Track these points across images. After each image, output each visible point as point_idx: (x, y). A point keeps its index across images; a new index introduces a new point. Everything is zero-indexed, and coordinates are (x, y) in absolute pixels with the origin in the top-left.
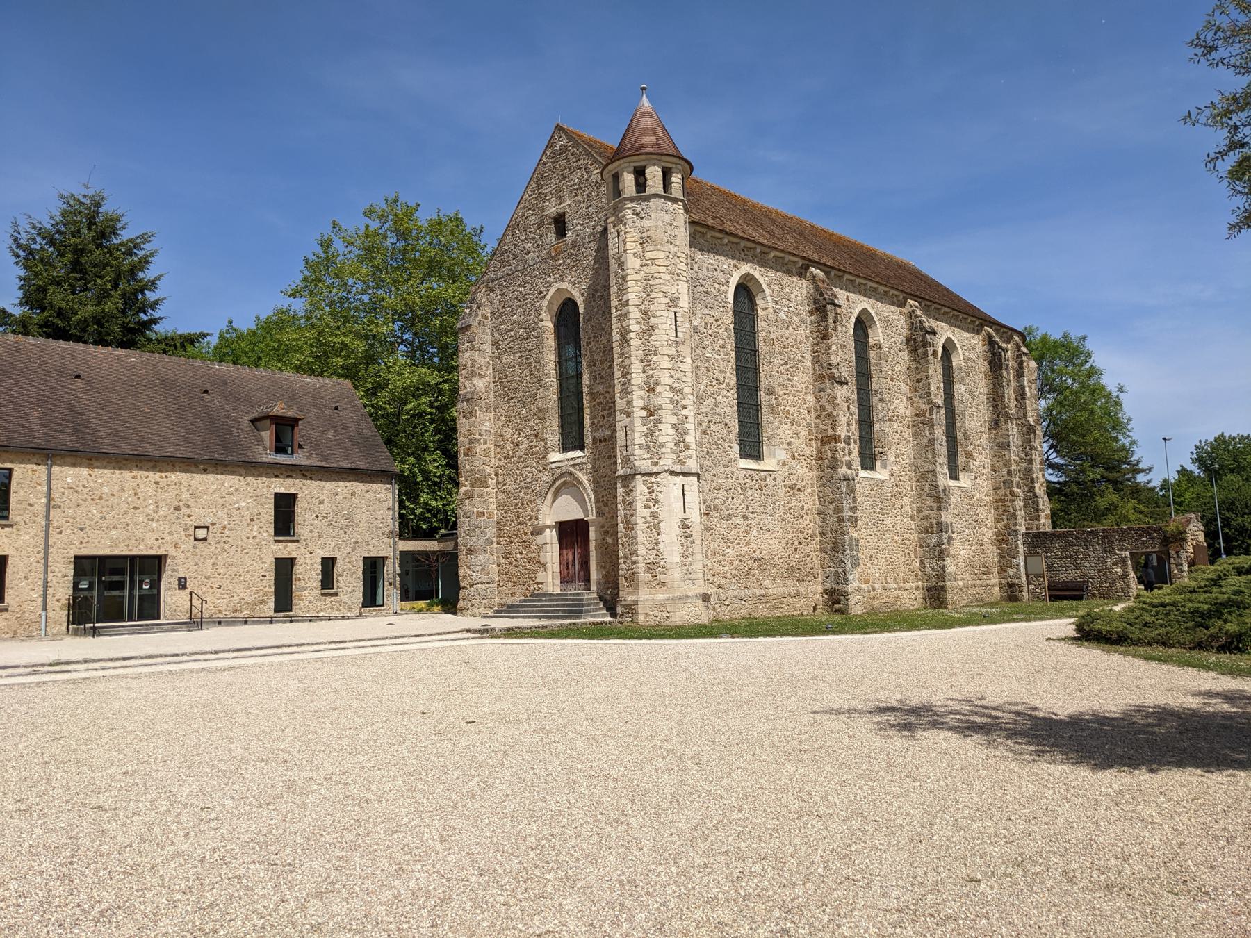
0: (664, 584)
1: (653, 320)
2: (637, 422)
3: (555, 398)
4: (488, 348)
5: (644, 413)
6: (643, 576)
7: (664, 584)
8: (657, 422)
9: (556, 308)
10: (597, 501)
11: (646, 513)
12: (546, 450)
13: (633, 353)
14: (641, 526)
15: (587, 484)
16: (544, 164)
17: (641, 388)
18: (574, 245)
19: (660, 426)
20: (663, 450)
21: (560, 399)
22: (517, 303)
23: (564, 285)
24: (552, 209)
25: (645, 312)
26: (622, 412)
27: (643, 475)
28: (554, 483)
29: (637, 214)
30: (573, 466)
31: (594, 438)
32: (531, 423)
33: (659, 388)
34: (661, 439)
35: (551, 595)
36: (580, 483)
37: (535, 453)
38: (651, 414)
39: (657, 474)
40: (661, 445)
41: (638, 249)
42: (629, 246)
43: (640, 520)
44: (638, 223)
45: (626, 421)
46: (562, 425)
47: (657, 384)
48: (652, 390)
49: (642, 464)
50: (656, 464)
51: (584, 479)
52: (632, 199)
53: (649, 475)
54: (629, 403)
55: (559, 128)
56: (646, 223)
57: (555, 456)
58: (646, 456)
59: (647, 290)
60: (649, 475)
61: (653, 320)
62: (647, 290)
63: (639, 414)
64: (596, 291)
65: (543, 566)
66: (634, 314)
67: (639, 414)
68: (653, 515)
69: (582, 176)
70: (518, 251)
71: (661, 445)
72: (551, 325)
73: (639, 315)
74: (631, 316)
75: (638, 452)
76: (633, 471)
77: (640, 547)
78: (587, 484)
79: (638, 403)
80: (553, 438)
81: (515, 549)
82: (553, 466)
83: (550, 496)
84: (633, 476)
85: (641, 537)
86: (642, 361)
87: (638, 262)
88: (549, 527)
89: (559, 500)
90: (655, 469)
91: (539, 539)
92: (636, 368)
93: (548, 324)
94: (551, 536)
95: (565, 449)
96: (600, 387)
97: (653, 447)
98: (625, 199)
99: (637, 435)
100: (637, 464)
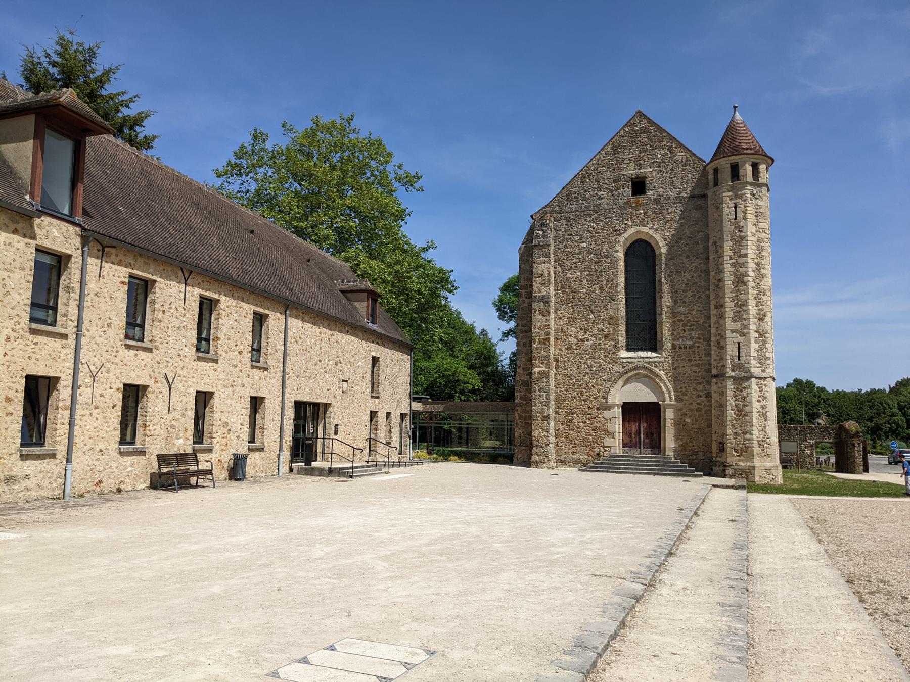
0: (769, 456)
1: (763, 271)
2: (752, 340)
3: (624, 310)
4: (552, 263)
5: (757, 335)
6: (756, 450)
7: (769, 456)
8: (765, 342)
9: (628, 244)
10: (675, 391)
11: (758, 405)
12: (617, 347)
13: (750, 291)
14: (755, 415)
15: (665, 377)
16: (622, 136)
17: (755, 317)
18: (657, 201)
19: (767, 346)
20: (769, 362)
21: (627, 312)
22: (586, 234)
23: (646, 230)
24: (631, 171)
25: (758, 264)
26: (732, 331)
27: (756, 378)
28: (626, 373)
29: (754, 195)
30: (649, 363)
31: (674, 346)
32: (601, 325)
33: (766, 319)
34: (768, 355)
35: (617, 456)
36: (657, 375)
37: (605, 349)
38: (761, 336)
39: (765, 378)
40: (767, 359)
41: (754, 219)
42: (749, 216)
43: (755, 410)
44: (754, 201)
45: (741, 339)
46: (627, 331)
47: (765, 315)
48: (761, 320)
49: (756, 371)
50: (764, 371)
51: (662, 373)
52: (751, 184)
53: (760, 378)
54: (745, 327)
55: (640, 114)
56: (760, 203)
57: (624, 354)
58: (758, 365)
59: (760, 249)
60: (760, 378)
61: (763, 271)
62: (760, 249)
63: (754, 335)
64: (681, 239)
65: (612, 435)
66: (751, 265)
67: (754, 335)
68: (763, 407)
69: (666, 154)
70: (587, 195)
71: (767, 359)
72: (623, 256)
73: (754, 266)
74: (750, 265)
75: (753, 362)
76: (748, 375)
77: (754, 428)
78: (665, 377)
79: (753, 327)
80: (622, 340)
81: (577, 419)
82: (625, 361)
83: (620, 383)
84: (748, 378)
85: (755, 422)
86: (755, 298)
87: (754, 229)
88: (617, 405)
89: (629, 386)
90: (764, 375)
91: (607, 414)
92: (752, 302)
93: (621, 255)
94: (618, 412)
95: (628, 349)
96: (682, 309)
97: (763, 360)
98: (747, 183)
99: (752, 350)
100: (753, 370)
